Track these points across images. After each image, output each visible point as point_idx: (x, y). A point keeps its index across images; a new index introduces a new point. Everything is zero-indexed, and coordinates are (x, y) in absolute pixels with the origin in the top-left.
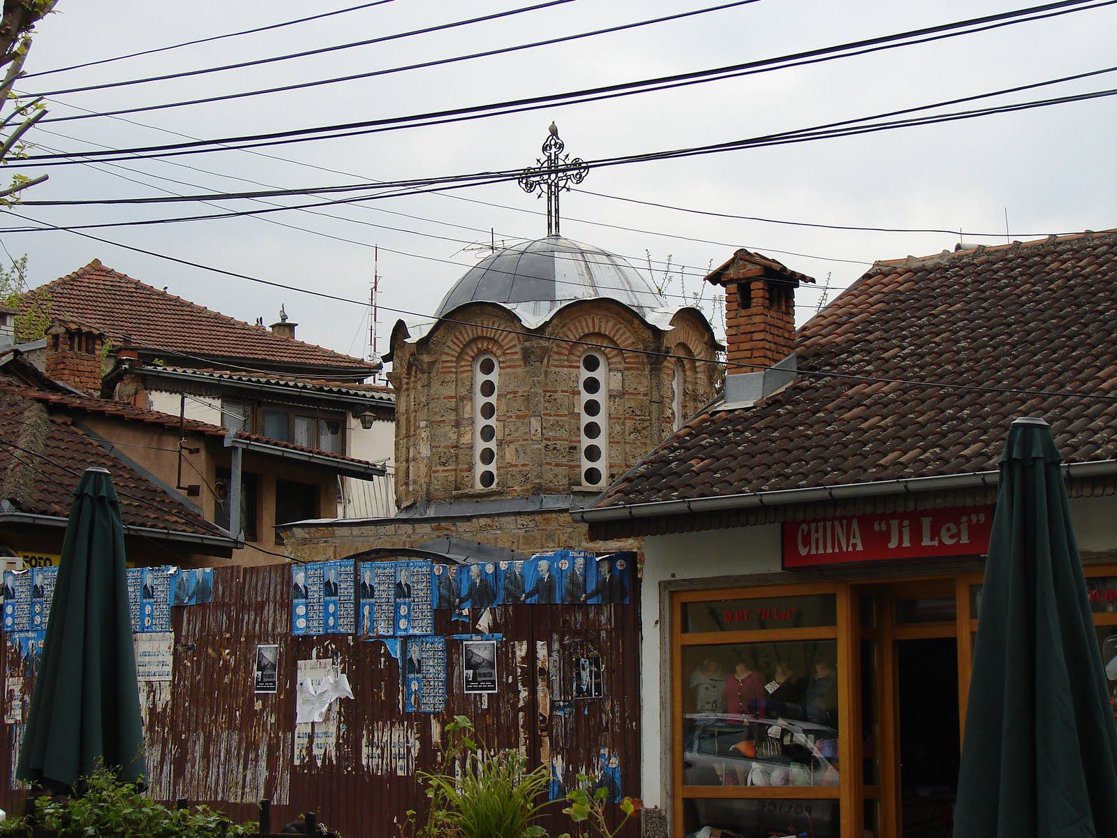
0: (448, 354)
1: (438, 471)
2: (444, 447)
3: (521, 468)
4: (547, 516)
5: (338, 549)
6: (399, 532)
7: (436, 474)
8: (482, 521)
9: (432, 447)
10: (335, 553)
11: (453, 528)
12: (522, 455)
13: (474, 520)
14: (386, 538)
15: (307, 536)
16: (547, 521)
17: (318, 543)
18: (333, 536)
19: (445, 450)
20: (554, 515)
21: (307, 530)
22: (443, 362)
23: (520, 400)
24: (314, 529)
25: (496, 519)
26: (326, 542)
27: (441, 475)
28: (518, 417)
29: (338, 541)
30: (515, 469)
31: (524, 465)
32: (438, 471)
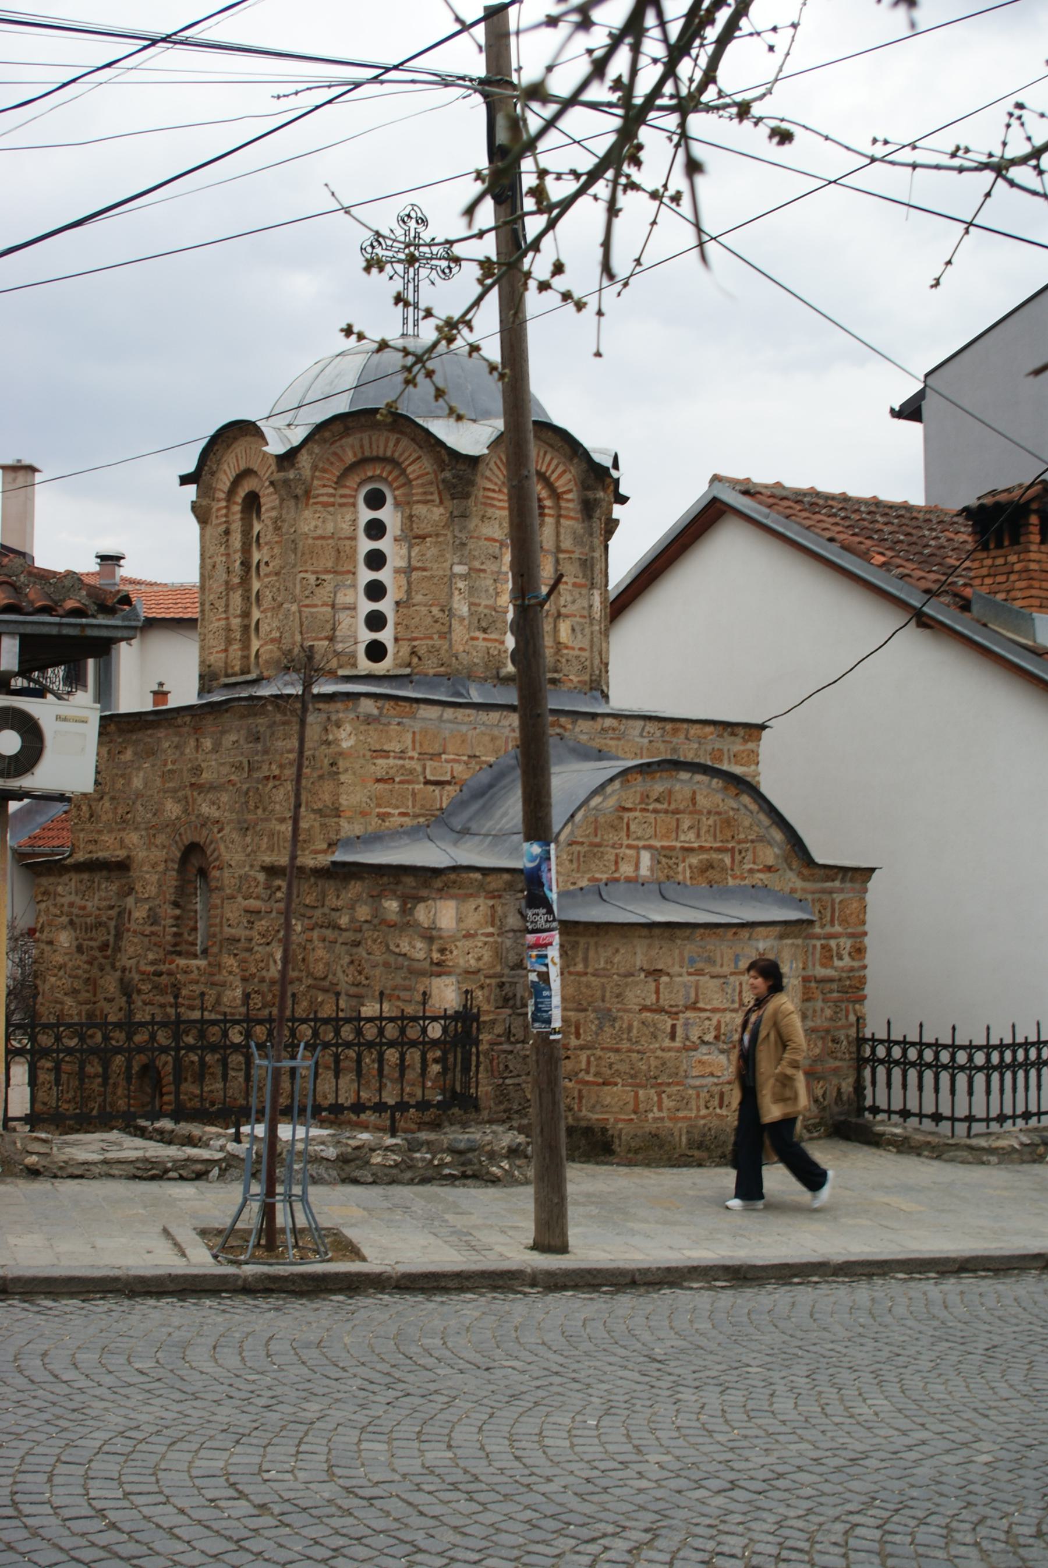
0: (490, 480)
1: (477, 639)
2: (486, 607)
3: (577, 652)
4: (678, 725)
5: (418, 737)
6: (505, 723)
7: (475, 643)
8: (608, 722)
9: (471, 604)
10: (414, 742)
11: (569, 726)
12: (580, 636)
13: (599, 719)
14: (483, 728)
15: (376, 712)
16: (675, 731)
17: (389, 723)
18: (413, 717)
19: (486, 611)
20: (685, 726)
21: (380, 704)
22: (485, 489)
23: (577, 564)
24: (392, 703)
25: (624, 721)
26: (399, 724)
27: (480, 643)
28: (575, 585)
29: (417, 726)
30: (571, 652)
31: (581, 649)
32: (477, 639)
